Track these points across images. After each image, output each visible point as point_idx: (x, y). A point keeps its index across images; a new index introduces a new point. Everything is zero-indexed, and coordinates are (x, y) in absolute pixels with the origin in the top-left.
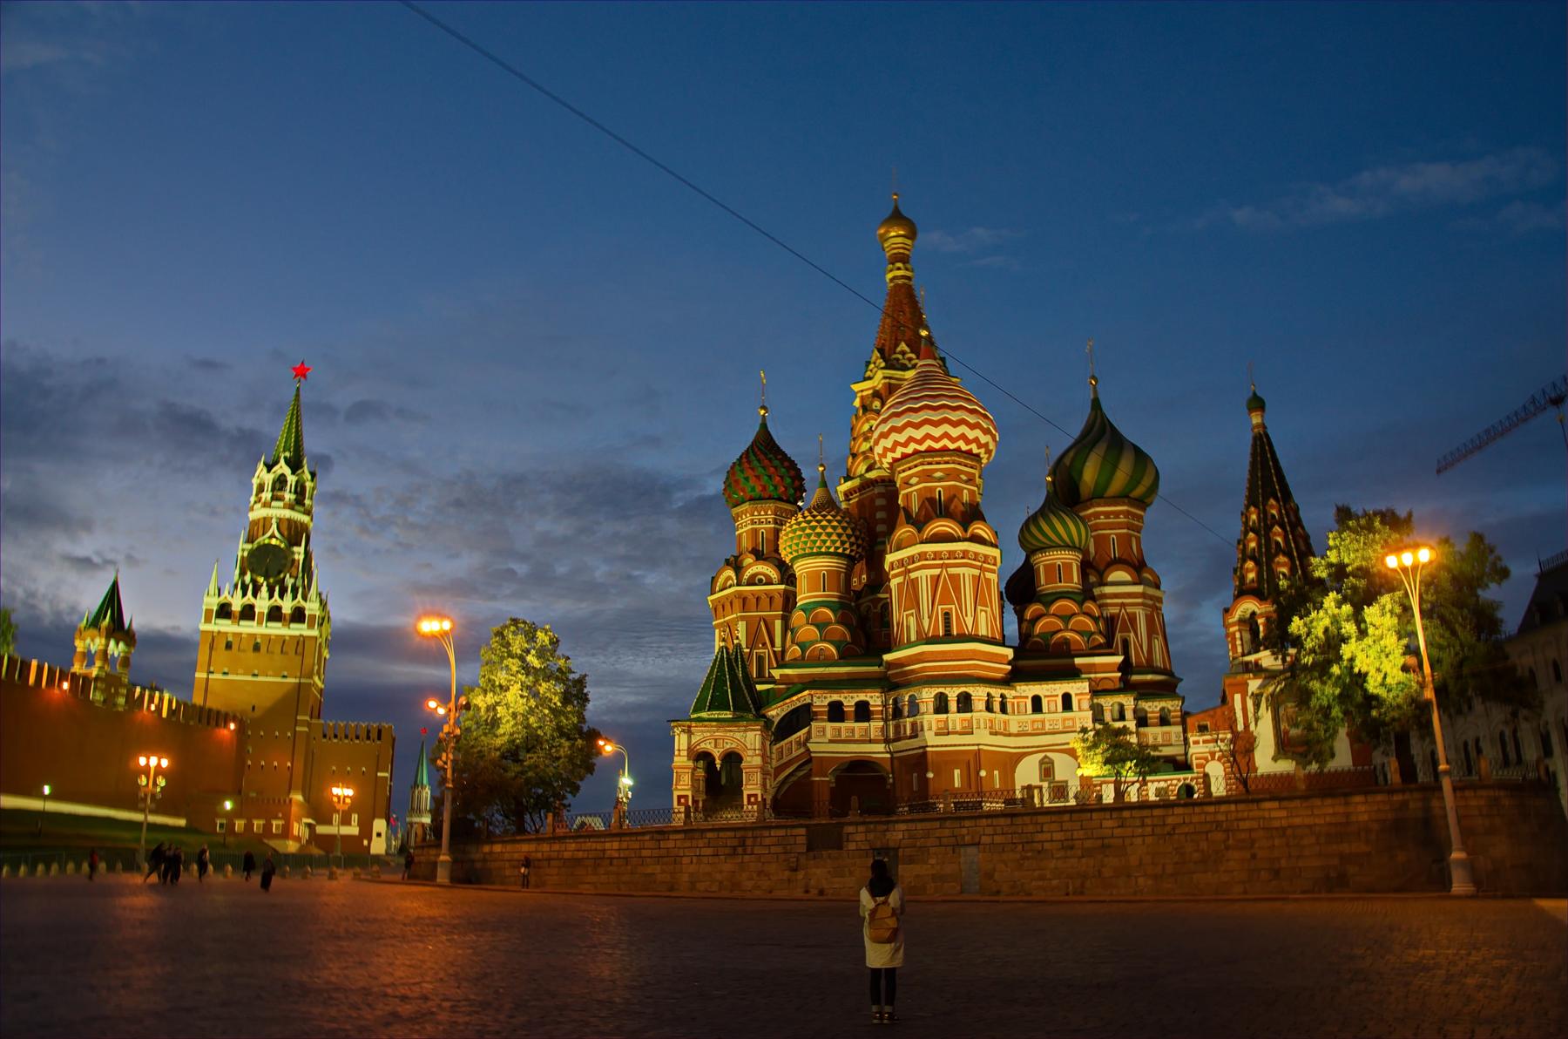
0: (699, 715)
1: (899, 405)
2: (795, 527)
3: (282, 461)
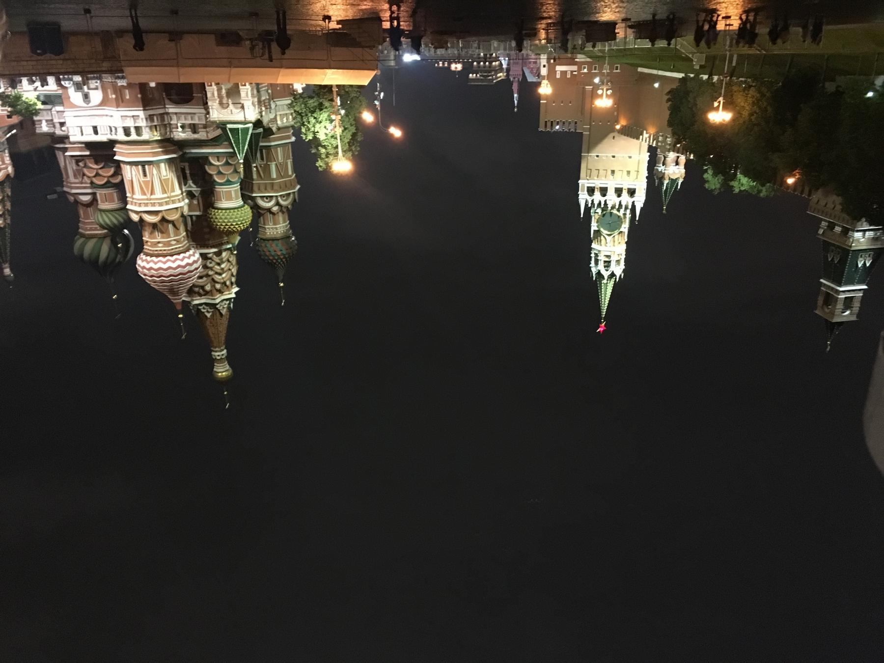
3: (606, 277)
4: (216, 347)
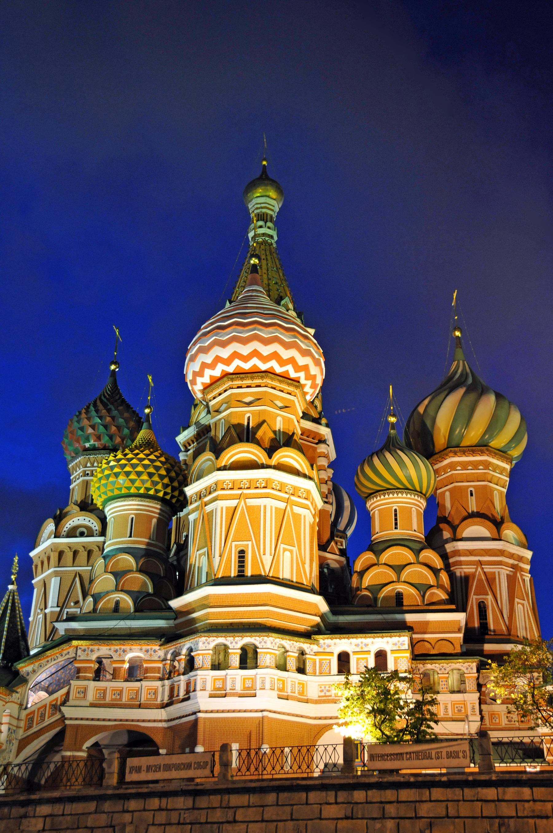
4: (265, 242)
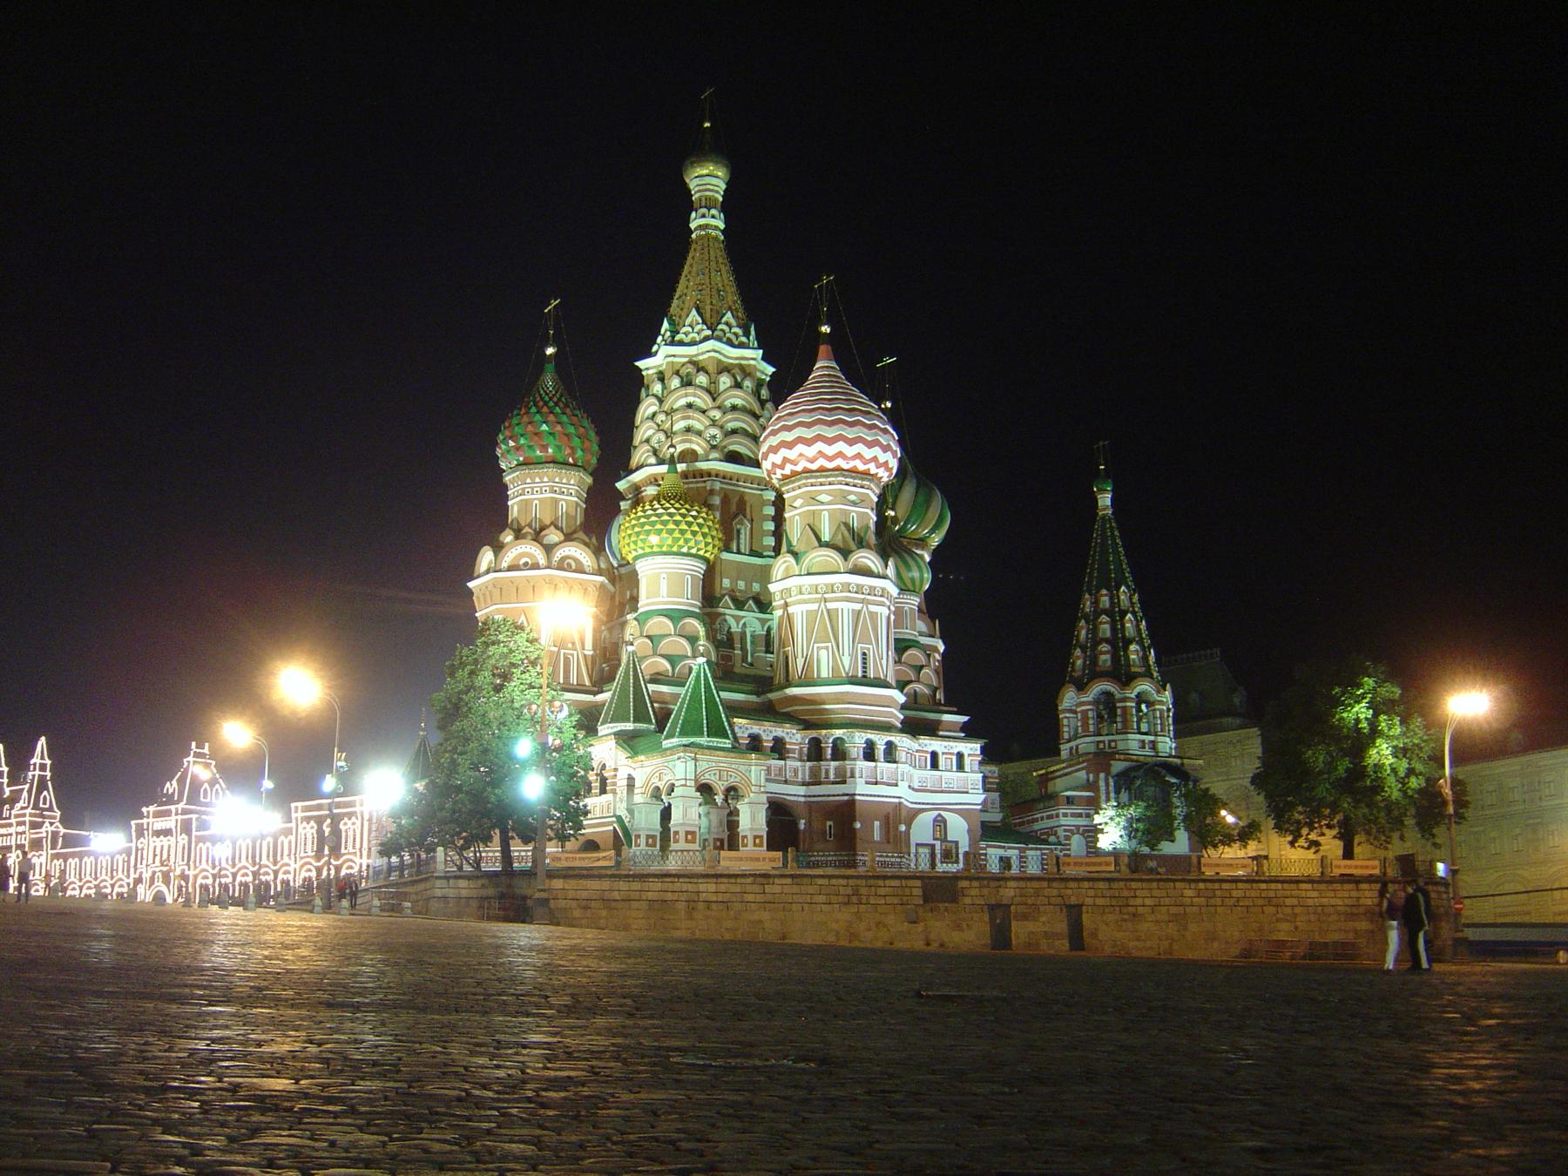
0: (692, 740)
1: (827, 413)
2: (666, 518)
4: (716, 238)
